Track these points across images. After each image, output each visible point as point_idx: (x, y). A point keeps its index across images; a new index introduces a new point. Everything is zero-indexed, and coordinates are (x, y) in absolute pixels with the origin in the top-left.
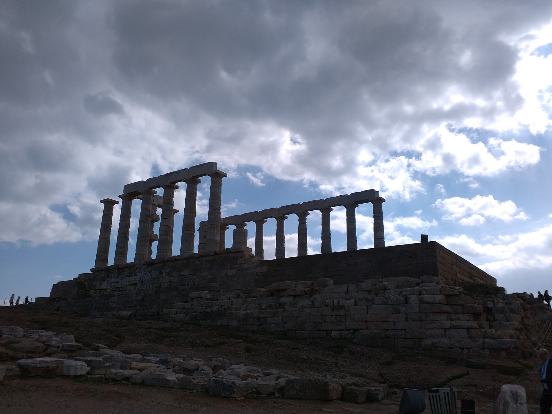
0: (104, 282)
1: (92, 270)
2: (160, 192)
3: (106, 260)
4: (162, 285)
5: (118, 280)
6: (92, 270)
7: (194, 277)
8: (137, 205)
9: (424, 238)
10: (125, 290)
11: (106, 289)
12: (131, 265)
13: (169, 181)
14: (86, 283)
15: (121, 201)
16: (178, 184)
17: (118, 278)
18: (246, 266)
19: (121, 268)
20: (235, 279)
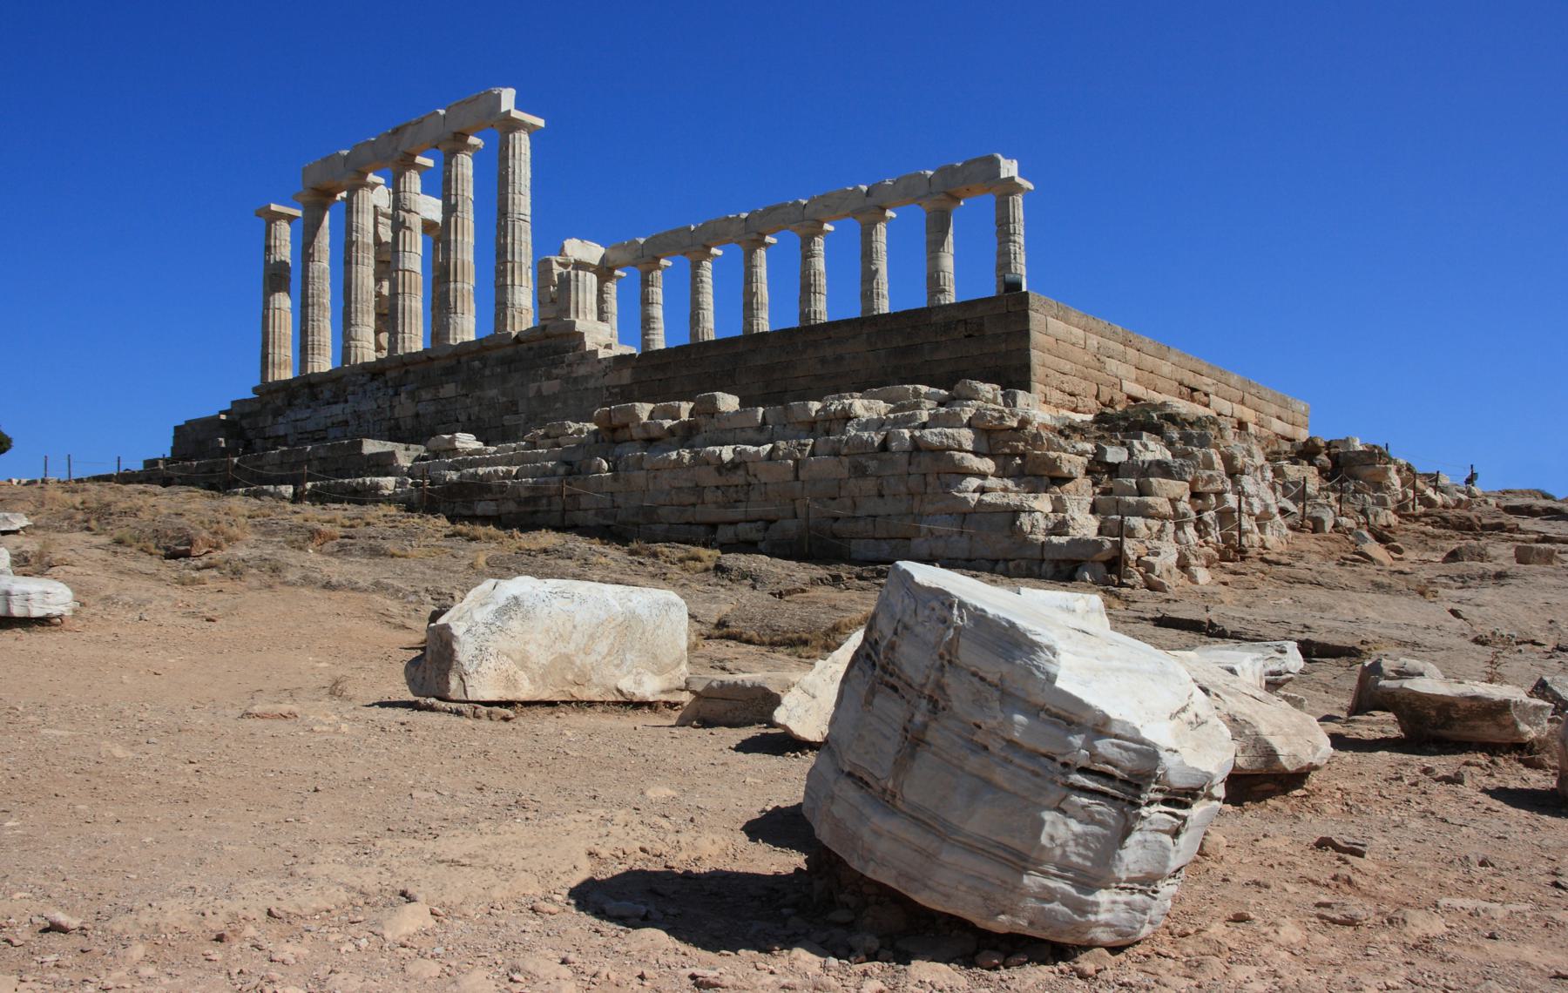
0: (280, 419)
1: (255, 390)
6: (255, 390)
14: (244, 423)
18: (582, 371)
20: (558, 405)
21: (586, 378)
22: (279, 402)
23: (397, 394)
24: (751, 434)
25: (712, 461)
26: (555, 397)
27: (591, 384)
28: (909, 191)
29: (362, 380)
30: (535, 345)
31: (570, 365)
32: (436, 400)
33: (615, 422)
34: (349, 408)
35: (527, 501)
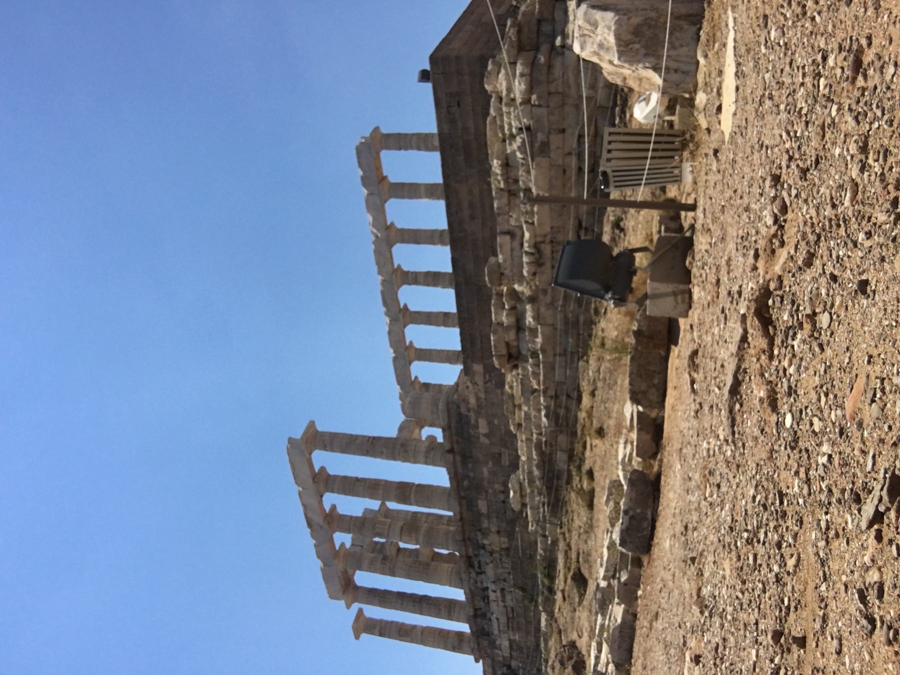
0: (498, 643)
1: (477, 661)
2: (343, 539)
3: (460, 634)
4: (504, 546)
5: (493, 618)
6: (477, 661)
7: (490, 491)
8: (364, 579)
9: (425, 76)
10: (512, 608)
11: (510, 640)
12: (471, 595)
13: (324, 524)
15: (356, 606)
16: (327, 508)
17: (490, 619)
18: (472, 401)
19: (477, 612)
20: (496, 422)
21: (478, 399)
22: (486, 643)
23: (483, 547)
24: (516, 244)
25: (533, 270)
26: (490, 423)
27: (482, 395)
28: (376, 207)
29: (473, 575)
30: (455, 438)
31: (469, 411)
32: (488, 516)
33: (504, 351)
34: (492, 587)
35: (557, 424)
